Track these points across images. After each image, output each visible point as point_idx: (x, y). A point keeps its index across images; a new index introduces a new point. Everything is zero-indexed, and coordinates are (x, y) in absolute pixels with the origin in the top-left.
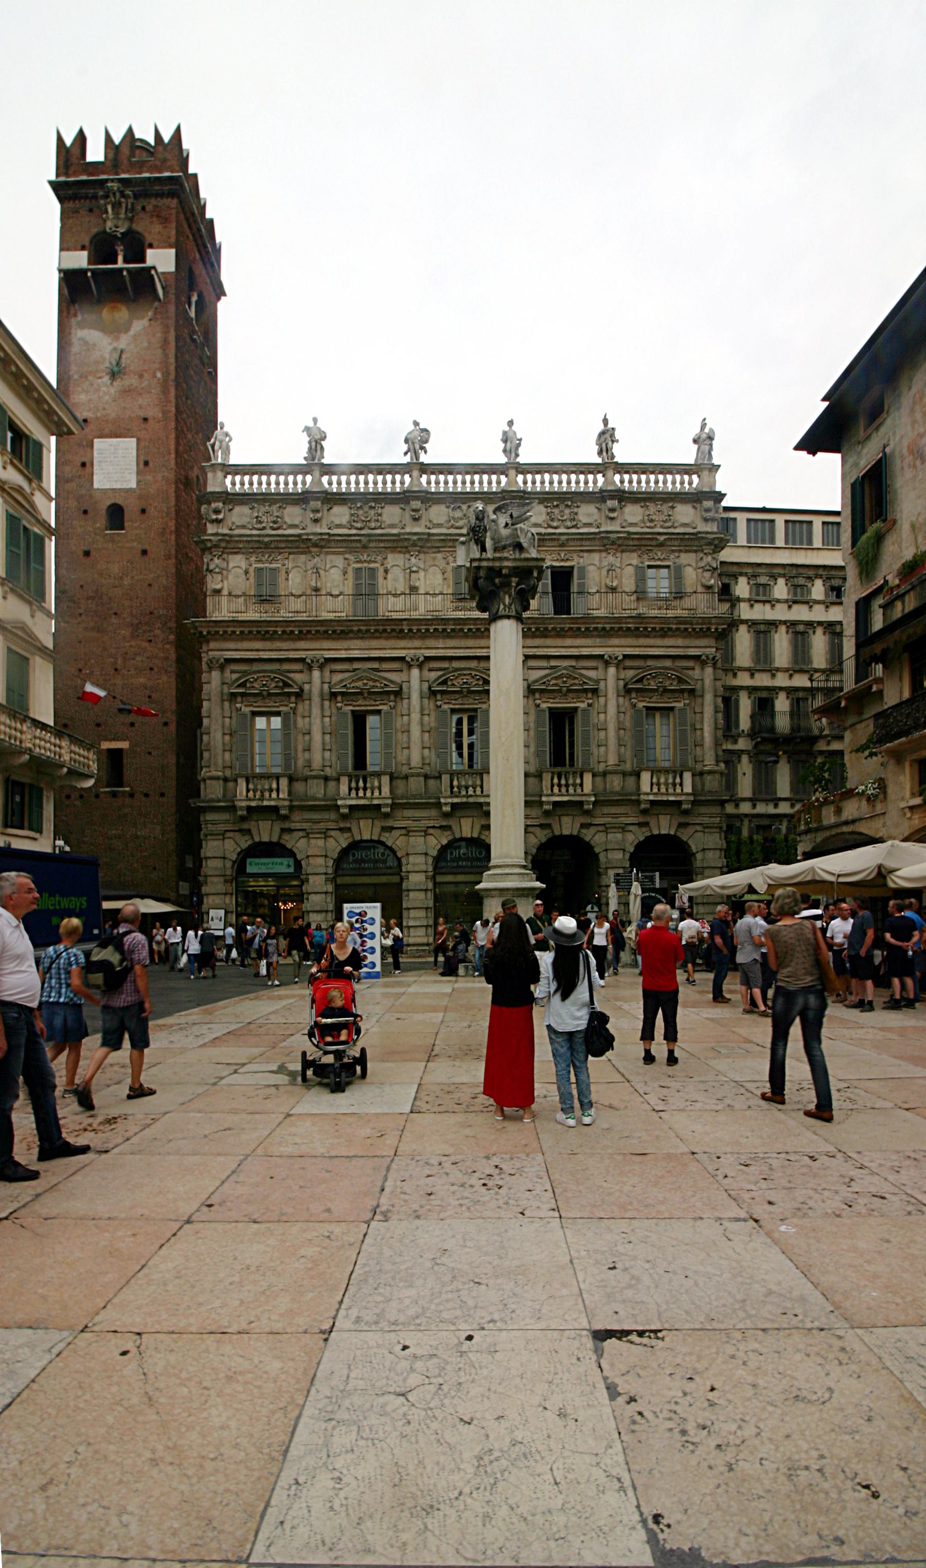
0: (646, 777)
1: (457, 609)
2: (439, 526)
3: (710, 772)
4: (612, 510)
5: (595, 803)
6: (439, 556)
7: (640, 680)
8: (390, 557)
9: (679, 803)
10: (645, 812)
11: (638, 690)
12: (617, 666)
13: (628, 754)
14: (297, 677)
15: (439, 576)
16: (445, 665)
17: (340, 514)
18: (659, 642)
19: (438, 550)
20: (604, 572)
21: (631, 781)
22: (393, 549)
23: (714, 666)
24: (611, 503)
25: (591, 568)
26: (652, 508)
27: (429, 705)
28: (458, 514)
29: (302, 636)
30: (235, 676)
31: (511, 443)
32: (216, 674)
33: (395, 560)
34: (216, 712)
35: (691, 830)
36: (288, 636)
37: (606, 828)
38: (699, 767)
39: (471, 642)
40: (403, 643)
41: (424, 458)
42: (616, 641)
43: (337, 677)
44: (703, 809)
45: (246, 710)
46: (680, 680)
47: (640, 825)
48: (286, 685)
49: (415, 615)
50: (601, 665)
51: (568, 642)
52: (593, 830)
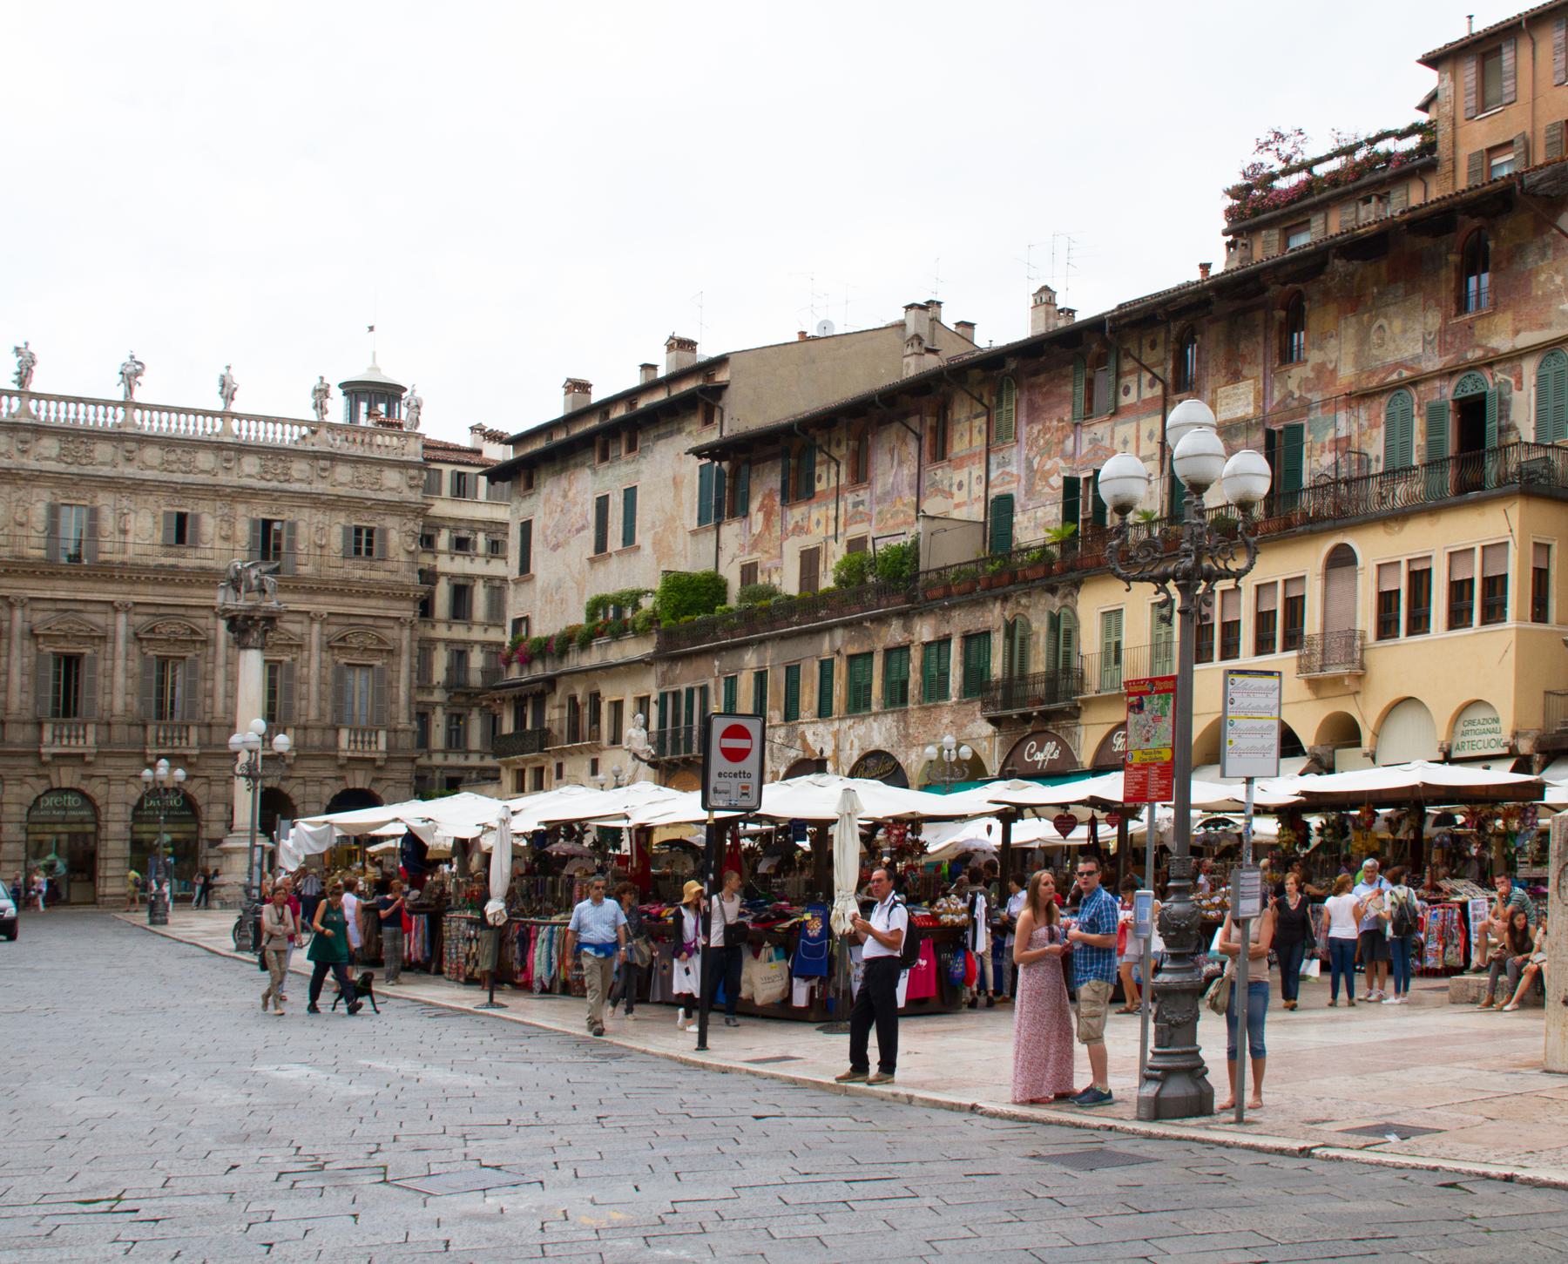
0: (344, 735)
1: (166, 555)
2: (153, 468)
3: (403, 731)
4: (324, 470)
5: (296, 758)
6: (151, 498)
7: (343, 639)
8: (101, 495)
9: (373, 760)
10: (342, 767)
11: (340, 648)
12: (321, 623)
13: (329, 708)
15: (150, 520)
16: (152, 610)
17: (50, 446)
18: (361, 602)
19: (150, 492)
20: (313, 529)
21: (330, 735)
22: (103, 488)
23: (412, 628)
24: (322, 463)
25: (301, 524)
26: (363, 469)
27: (135, 649)
28: (172, 457)
31: (227, 390)
33: (105, 501)
35: (384, 784)
37: (305, 781)
38: (393, 723)
39: (180, 591)
40: (111, 587)
42: (322, 599)
44: (396, 766)
46: (380, 641)
47: (337, 778)
49: (125, 558)
50: (306, 621)
52: (293, 782)
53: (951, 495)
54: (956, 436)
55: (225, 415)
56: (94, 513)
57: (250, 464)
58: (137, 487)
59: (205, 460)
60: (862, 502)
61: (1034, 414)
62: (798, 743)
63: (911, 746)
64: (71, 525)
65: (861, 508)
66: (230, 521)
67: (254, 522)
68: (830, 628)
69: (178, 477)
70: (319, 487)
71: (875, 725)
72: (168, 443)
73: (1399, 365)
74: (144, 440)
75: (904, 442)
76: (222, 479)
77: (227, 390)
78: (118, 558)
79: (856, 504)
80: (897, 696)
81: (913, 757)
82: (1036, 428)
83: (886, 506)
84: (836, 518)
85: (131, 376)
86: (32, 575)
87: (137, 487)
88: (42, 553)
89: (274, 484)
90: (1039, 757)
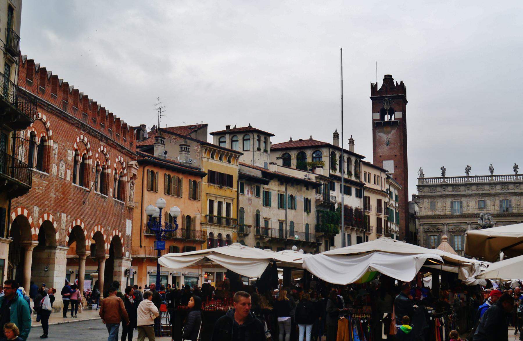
14: (441, 227)
24: (517, 185)
29: (442, 218)
30: (426, 227)
31: (491, 170)
32: (421, 227)
33: (464, 200)
34: (422, 235)
36: (439, 218)
41: (470, 175)
42: (520, 218)
43: (450, 227)
45: (429, 235)
48: (438, 229)
49: (469, 212)
51: (507, 218)
55: (492, 176)
56: (461, 203)
57: (498, 187)
58: (471, 196)
59: (487, 187)
64: (457, 206)
66: (494, 201)
67: (501, 201)
69: (481, 192)
70: (517, 191)
72: (477, 184)
74: (472, 185)
76: (492, 191)
77: (491, 170)
78: (466, 212)
85: (468, 169)
86: (448, 218)
87: (471, 196)
88: (450, 213)
89: (505, 191)
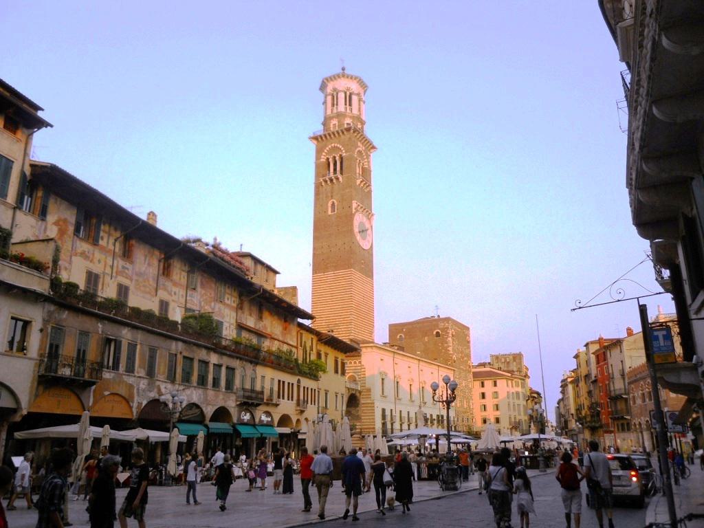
53: (172, 296)
54: (175, 273)
60: (128, 269)
61: (203, 286)
62: (156, 390)
63: (208, 404)
65: (126, 271)
68: (177, 339)
71: (194, 392)
73: (276, 335)
75: (152, 256)
79: (123, 267)
80: (202, 381)
81: (209, 409)
82: (203, 292)
83: (141, 279)
84: (112, 267)
90: (245, 417)
